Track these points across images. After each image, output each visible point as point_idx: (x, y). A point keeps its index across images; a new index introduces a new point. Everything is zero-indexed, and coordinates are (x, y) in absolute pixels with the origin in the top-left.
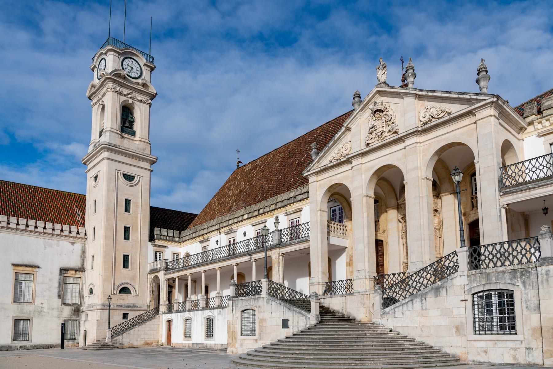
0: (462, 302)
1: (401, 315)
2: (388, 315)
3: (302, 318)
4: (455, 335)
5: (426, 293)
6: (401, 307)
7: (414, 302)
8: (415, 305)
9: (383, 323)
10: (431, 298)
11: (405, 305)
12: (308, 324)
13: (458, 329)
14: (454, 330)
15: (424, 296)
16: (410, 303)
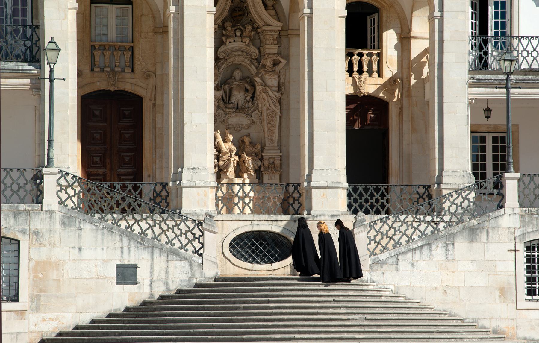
0: (510, 253)
1: (409, 267)
2: (385, 267)
3: (178, 263)
4: (498, 301)
5: (454, 235)
6: (409, 255)
7: (433, 247)
8: (434, 252)
9: (374, 279)
10: (461, 245)
11: (418, 252)
12: (198, 275)
13: (503, 291)
14: (497, 293)
15: (451, 240)
16: (426, 249)
